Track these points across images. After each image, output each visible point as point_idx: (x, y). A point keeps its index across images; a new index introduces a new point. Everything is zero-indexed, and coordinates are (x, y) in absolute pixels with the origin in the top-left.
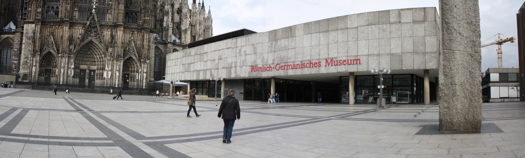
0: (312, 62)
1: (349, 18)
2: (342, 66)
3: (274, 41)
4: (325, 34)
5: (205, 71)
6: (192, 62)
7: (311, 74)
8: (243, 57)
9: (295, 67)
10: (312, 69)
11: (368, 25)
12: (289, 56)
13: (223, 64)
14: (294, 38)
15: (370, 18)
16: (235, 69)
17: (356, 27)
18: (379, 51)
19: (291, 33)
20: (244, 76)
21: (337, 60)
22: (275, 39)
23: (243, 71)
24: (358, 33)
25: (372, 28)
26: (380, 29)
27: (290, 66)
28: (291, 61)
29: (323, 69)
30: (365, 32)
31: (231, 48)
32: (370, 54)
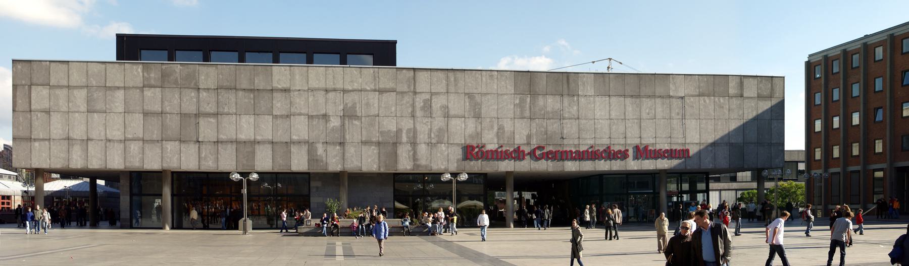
4: (634, 100)
5: (283, 146)
6: (210, 108)
8: (439, 122)
11: (699, 96)
13: (364, 133)
15: (702, 85)
20: (443, 167)
22: (530, 92)
23: (439, 155)
28: (571, 142)
30: (694, 105)
31: (393, 90)
32: (702, 142)
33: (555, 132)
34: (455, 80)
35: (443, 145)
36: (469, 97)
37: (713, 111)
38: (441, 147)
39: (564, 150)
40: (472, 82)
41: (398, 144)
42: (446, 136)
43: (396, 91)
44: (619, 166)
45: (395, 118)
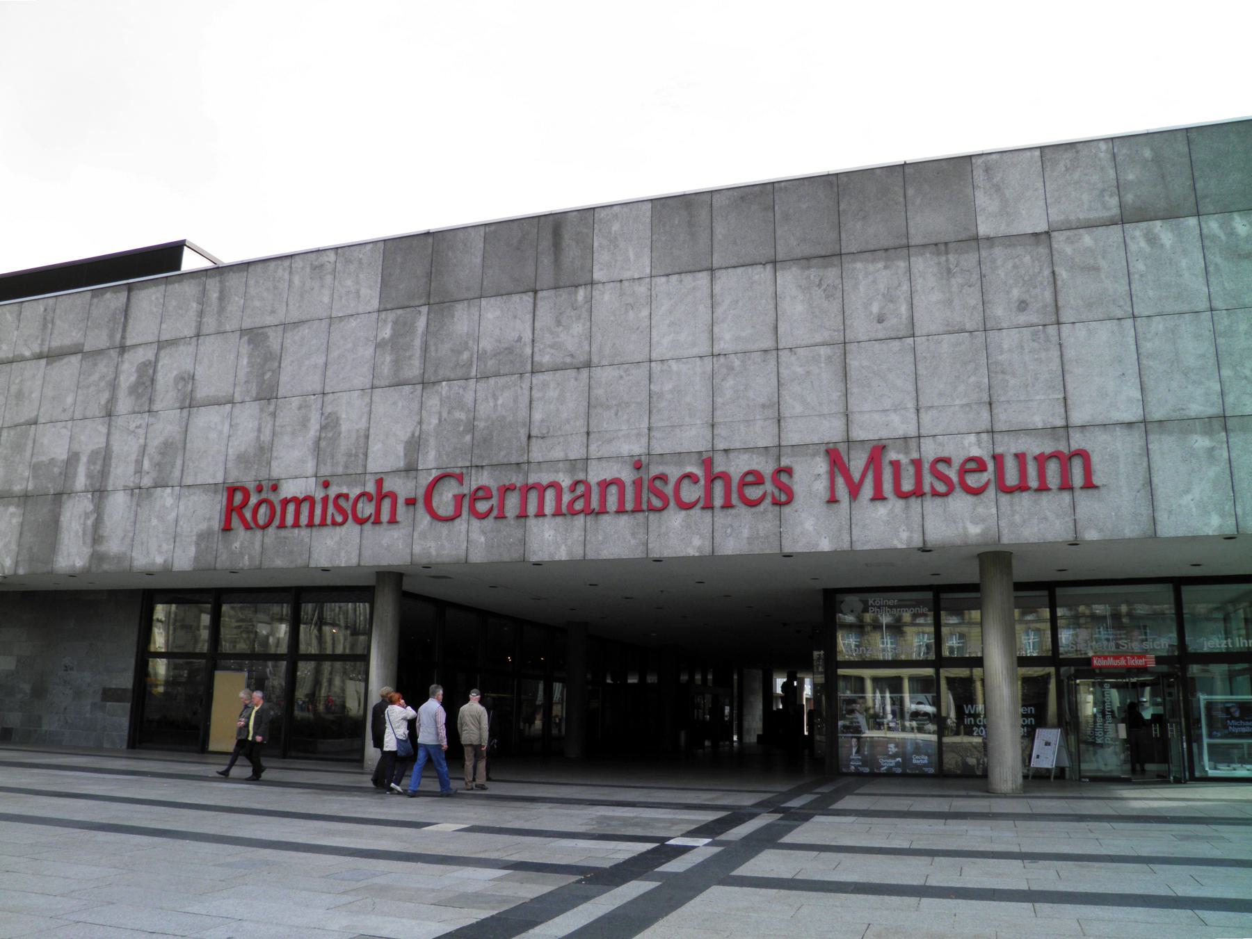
0: (718, 468)
1: (979, 175)
2: (960, 503)
3: (425, 309)
4: (813, 273)
7: (711, 560)
8: (166, 425)
9: (588, 503)
10: (722, 518)
11: (1122, 220)
12: (537, 416)
14: (581, 294)
15: (1131, 177)
16: (90, 507)
17: (1036, 235)
18: (1222, 393)
19: (557, 261)
20: (159, 560)
21: (915, 456)
22: (429, 297)
23: (154, 522)
24: (1053, 273)
25: (1152, 240)
26: (1207, 243)
27: (550, 495)
28: (558, 454)
29: (809, 525)
30: (1103, 263)
32: (1157, 416)
33: (504, 418)
34: (221, 298)
35: (169, 490)
36: (249, 342)
37: (1202, 280)
38: (162, 497)
39: (531, 481)
40: (265, 294)
41: (65, 497)
42: (179, 462)
43: (81, 352)
44: (750, 540)
45: (70, 423)
